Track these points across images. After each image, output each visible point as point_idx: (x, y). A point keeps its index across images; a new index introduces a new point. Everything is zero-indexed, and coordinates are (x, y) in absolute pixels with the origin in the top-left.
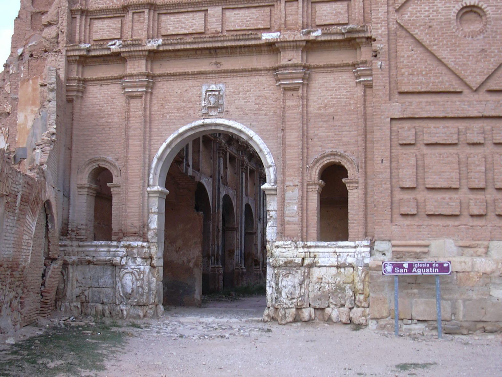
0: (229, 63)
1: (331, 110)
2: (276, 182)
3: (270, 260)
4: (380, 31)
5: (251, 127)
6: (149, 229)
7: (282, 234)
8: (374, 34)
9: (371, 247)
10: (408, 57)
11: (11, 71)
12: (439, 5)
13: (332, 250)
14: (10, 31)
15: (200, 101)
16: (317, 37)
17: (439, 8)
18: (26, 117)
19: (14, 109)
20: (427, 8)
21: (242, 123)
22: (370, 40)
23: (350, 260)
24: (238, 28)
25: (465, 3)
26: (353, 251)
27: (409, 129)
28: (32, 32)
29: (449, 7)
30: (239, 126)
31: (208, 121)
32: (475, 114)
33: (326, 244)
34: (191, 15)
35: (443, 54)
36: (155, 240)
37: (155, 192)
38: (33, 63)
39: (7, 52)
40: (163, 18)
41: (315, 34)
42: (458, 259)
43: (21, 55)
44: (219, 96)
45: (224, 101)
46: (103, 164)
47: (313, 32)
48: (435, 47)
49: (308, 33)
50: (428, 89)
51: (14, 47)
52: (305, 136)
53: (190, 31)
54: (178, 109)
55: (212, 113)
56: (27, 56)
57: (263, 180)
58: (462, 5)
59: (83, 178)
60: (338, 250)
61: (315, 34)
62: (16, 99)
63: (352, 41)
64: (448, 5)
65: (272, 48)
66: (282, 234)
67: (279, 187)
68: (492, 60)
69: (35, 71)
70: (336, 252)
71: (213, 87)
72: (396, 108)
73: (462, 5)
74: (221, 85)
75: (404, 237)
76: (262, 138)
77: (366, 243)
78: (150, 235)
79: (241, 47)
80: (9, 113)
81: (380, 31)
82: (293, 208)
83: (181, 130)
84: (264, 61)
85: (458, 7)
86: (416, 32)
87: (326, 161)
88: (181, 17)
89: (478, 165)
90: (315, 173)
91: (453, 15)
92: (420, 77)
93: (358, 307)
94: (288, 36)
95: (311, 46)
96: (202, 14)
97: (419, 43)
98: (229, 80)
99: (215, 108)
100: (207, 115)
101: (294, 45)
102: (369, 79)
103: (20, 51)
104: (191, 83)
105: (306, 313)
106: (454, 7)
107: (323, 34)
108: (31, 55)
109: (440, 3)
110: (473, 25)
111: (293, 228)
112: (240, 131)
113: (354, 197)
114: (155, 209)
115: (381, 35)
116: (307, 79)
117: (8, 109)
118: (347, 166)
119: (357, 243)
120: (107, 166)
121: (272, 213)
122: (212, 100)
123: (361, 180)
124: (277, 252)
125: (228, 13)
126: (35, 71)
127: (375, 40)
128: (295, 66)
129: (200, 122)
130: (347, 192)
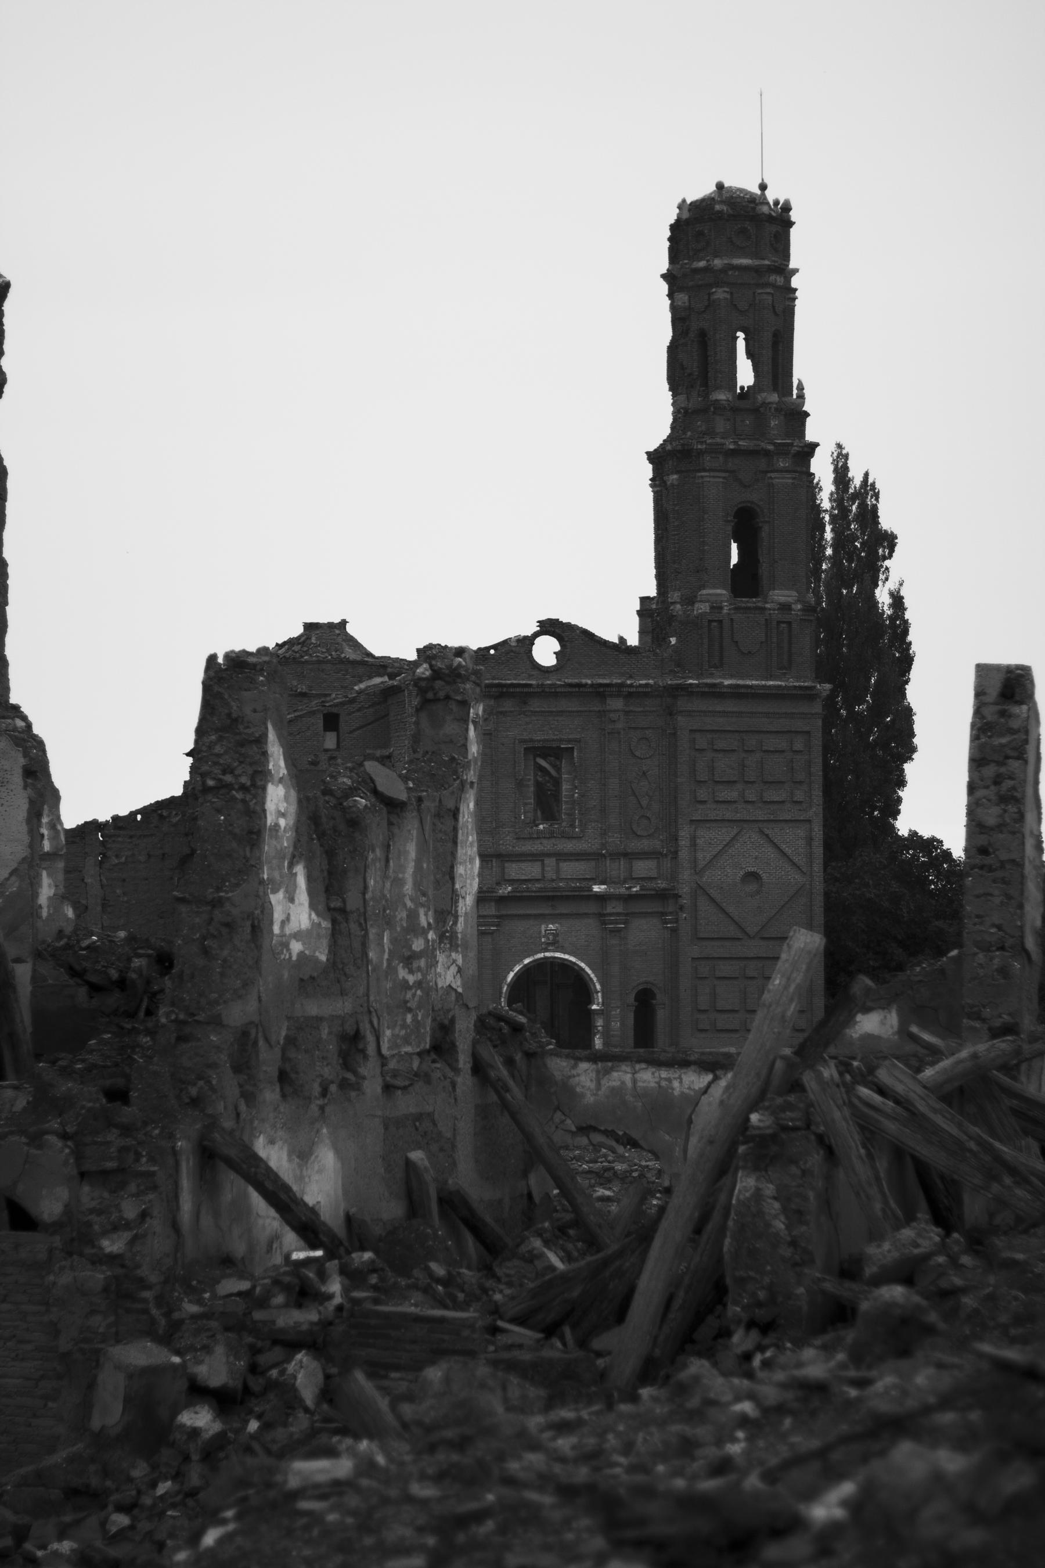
0: (563, 909)
5: (582, 961)
8: (680, 893)
15: (540, 938)
22: (677, 896)
30: (573, 959)
31: (548, 954)
32: (752, 955)
35: (731, 909)
40: (506, 865)
45: (560, 938)
53: (529, 877)
63: (663, 896)
65: (600, 898)
76: (591, 969)
82: (616, 1025)
83: (527, 961)
84: (592, 908)
86: (713, 892)
88: (523, 865)
90: (631, 999)
96: (539, 863)
97: (712, 900)
99: (552, 944)
101: (619, 898)
107: (641, 889)
110: (752, 887)
118: (656, 991)
125: (561, 864)
128: (618, 914)
129: (541, 955)
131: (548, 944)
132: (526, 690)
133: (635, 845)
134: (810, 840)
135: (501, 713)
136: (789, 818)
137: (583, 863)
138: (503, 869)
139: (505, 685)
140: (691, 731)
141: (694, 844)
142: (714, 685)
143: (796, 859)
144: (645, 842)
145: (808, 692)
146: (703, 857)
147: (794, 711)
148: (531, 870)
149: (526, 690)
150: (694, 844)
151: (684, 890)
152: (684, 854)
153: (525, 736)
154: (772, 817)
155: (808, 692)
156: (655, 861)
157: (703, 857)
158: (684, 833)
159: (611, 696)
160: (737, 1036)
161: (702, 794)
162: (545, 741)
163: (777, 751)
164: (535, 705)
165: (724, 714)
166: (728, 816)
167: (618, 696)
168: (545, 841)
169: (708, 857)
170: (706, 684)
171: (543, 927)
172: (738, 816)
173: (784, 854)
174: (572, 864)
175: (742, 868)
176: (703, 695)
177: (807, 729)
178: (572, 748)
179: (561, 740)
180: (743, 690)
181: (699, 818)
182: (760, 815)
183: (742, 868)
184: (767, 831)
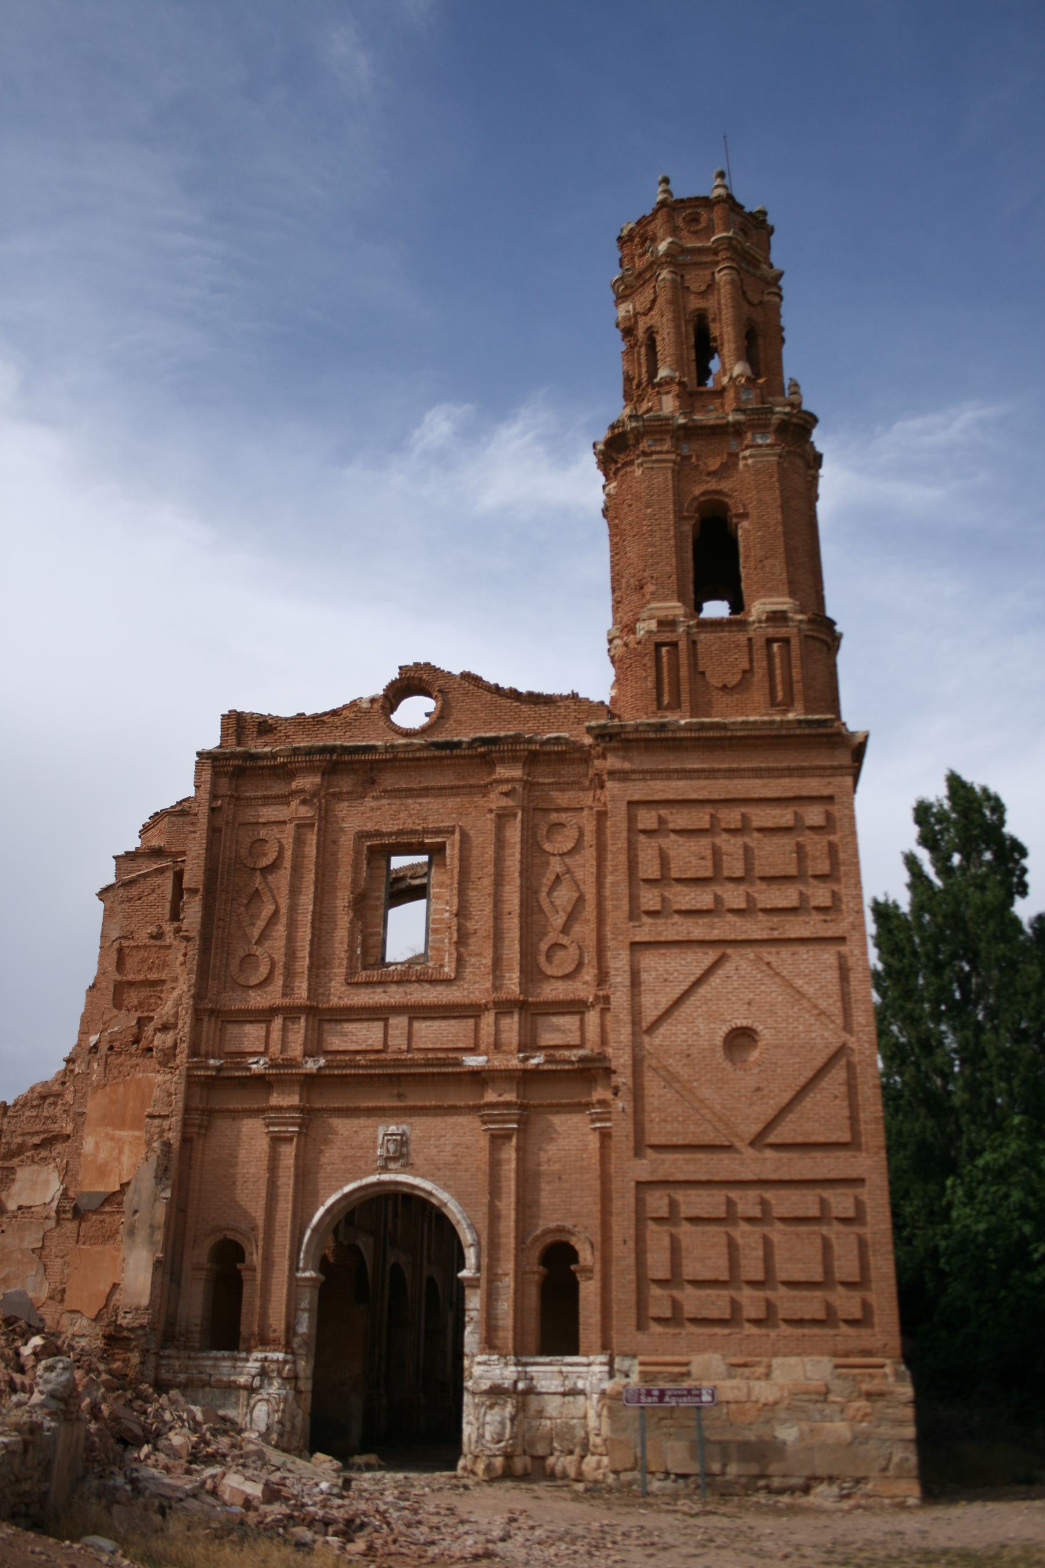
1: (557, 1167)
2: (478, 1269)
3: (469, 1384)
4: (622, 1061)
5: (446, 1187)
6: (295, 1334)
7: (490, 1344)
8: (614, 1065)
9: (610, 1363)
10: (661, 1096)
11: (77, 1070)
13: (555, 1368)
14: (79, 1004)
15: (375, 1148)
16: (538, 1065)
18: (97, 1144)
19: (77, 1129)
20: (685, 1030)
21: (433, 1181)
22: (609, 1072)
23: (580, 1384)
24: (430, 1046)
26: (589, 1371)
27: (661, 1198)
28: (115, 1012)
31: (386, 1177)
32: (750, 1176)
33: (547, 1359)
34: (365, 1024)
36: (302, 1351)
37: (306, 1279)
38: (113, 1060)
39: (74, 1041)
41: (534, 1061)
42: (729, 1383)
43: (95, 1046)
44: (403, 1142)
46: (230, 1235)
47: (533, 1057)
48: (695, 1084)
49: (526, 1059)
50: (687, 1142)
51: (84, 1033)
52: (526, 1206)
53: (363, 1047)
54: (344, 1158)
55: (392, 1166)
56: (104, 1048)
57: (462, 1266)
59: (200, 1255)
60: (564, 1369)
61: (534, 1061)
62: (82, 1114)
65: (480, 1078)
66: (490, 1344)
67: (483, 1275)
68: (771, 1102)
69: (115, 1072)
70: (561, 1372)
71: (393, 1129)
72: (643, 1168)
74: (404, 1127)
75: (655, 1352)
77: (603, 1358)
78: (296, 1342)
79: (433, 1074)
80: (68, 1136)
81: (622, 1061)
83: (347, 1189)
85: (725, 1029)
87: (549, 1239)
89: (755, 1249)
91: (719, 1040)
92: (676, 1125)
93: (593, 1454)
94: (499, 1062)
95: (526, 1078)
96: (381, 1024)
98: (414, 1119)
99: (395, 1159)
100: (385, 1169)
101: (507, 1076)
102: (608, 1124)
103: (93, 1039)
104: (363, 1121)
105: (520, 1463)
107: (547, 1062)
108: (111, 1048)
111: (506, 1336)
112: (430, 1194)
113: (589, 1290)
114: (304, 1304)
115: (624, 1066)
116: (524, 1123)
117: (69, 1129)
119: (592, 1358)
120: (238, 1238)
121: (473, 1314)
122: (392, 1147)
123: (598, 1268)
124: (477, 1370)
125: (416, 1025)
126: (115, 1072)
127: (615, 1072)
130: (576, 1284)
131: (388, 1159)
132: (368, 757)
135: (334, 795)
136: (806, 934)
137: (452, 1022)
138: (320, 1035)
139: (332, 750)
140: (630, 803)
141: (635, 982)
143: (823, 1004)
145: (822, 731)
146: (652, 1004)
147: (805, 764)
148: (363, 1036)
149: (368, 757)
150: (635, 982)
151: (621, 1059)
152: (620, 999)
153: (370, 827)
154: (776, 934)
155: (822, 731)
157: (652, 1004)
160: (727, 1331)
162: (400, 833)
164: (389, 780)
168: (393, 988)
169: (665, 1003)
171: (381, 1131)
174: (436, 1024)
175: (724, 1021)
177: (826, 792)
178: (444, 844)
179: (426, 832)
181: (647, 939)
182: (755, 928)
183: (724, 1021)
184: (767, 958)
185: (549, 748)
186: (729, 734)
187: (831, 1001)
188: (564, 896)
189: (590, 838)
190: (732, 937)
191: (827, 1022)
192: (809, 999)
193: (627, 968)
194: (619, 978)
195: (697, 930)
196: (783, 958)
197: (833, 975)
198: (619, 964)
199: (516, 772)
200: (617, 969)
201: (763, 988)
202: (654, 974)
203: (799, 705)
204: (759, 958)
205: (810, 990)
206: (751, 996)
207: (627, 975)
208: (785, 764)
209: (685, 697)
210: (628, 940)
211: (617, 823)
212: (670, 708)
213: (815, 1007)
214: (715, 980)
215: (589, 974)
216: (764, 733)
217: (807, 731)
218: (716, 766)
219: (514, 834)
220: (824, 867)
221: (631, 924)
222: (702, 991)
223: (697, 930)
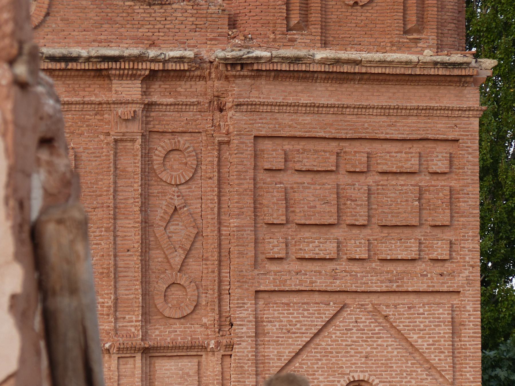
12: (321, 378)
17: (321, 382)
25: (353, 377)
29: (334, 381)
58: (348, 379)
64: (331, 378)
73: (348, 379)
106: (339, 382)
109: (322, 375)
133: (162, 334)
134: (455, 327)
136: (423, 287)
140: (256, 137)
141: (259, 332)
142: (297, 60)
144: (178, 327)
145: (456, 72)
147: (433, 104)
150: (259, 332)
152: (244, 349)
154: (394, 287)
155: (456, 72)
156: (195, 360)
158: (243, 315)
159: (121, 77)
161: (274, 245)
163: (401, 173)
165: (314, 108)
166: (320, 284)
167: (134, 77)
170: (284, 59)
172: (337, 285)
173: (413, 348)
175: (343, 374)
176: (278, 75)
180: (346, 68)
183: (343, 374)
184: (386, 311)
185: (171, 66)
186: (364, 70)
187: (442, 356)
188: (180, 231)
189: (208, 168)
190: (354, 288)
191: (437, 376)
192: (421, 354)
193: (252, 318)
194: (244, 329)
195: (318, 277)
196: (398, 309)
197: (445, 330)
198: (244, 314)
199: (131, 90)
200: (242, 319)
201: (380, 341)
202: (277, 324)
203: (430, 36)
204: (376, 310)
205: (422, 344)
206: (369, 349)
207: (252, 325)
208: (415, 104)
209: (315, 17)
210: (253, 289)
211: (240, 157)
212: (298, 27)
213: (427, 361)
214: (334, 332)
215: (208, 318)
216: (398, 71)
217: (441, 72)
218: (346, 102)
219: (131, 163)
220: (444, 218)
221: (256, 272)
222: (323, 342)
223: (318, 277)
